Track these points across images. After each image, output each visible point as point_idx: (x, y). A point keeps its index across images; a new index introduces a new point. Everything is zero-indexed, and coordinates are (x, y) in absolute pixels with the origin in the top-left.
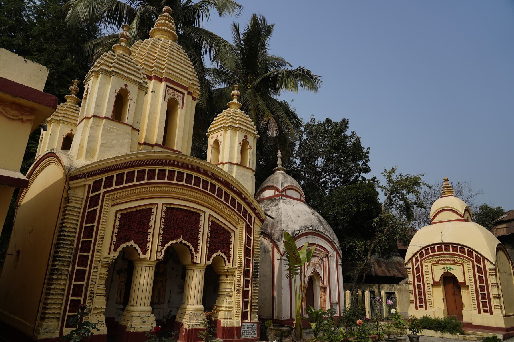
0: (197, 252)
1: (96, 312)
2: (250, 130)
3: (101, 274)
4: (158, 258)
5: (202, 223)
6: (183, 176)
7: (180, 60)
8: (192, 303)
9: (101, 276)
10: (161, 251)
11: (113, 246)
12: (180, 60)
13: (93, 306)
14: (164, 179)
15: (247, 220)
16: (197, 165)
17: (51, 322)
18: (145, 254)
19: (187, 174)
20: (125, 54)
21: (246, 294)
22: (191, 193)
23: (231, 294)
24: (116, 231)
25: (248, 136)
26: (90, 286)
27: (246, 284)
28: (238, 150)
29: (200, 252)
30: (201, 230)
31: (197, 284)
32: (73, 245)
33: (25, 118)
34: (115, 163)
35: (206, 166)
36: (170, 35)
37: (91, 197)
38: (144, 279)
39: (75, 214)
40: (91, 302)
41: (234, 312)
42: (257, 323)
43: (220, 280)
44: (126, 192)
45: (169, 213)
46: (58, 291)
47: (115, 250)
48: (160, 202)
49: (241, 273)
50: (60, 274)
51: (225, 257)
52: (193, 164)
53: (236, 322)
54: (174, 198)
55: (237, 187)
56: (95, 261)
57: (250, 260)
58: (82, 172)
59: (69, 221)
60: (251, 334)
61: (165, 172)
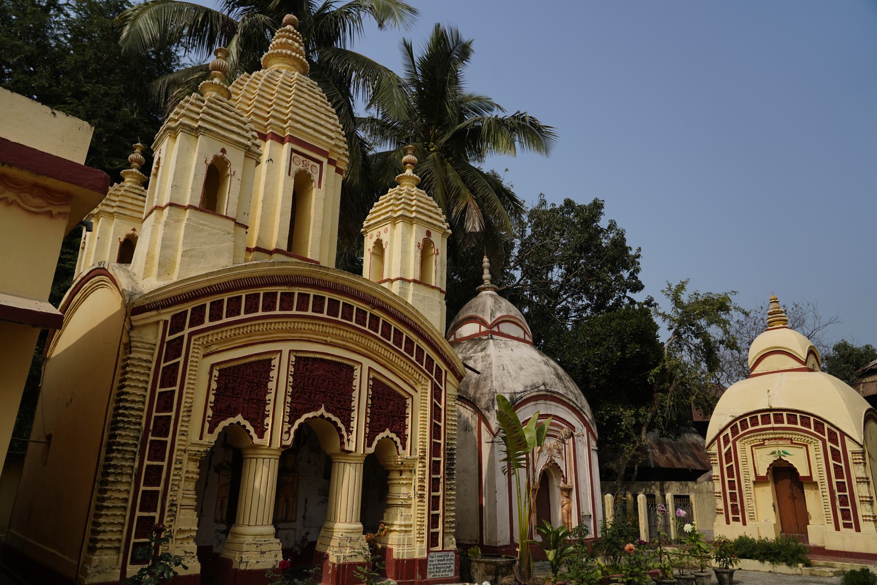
0: (349, 431)
1: (181, 536)
2: (435, 222)
3: (187, 472)
4: (284, 443)
5: (356, 383)
6: (323, 303)
7: (314, 106)
8: (343, 520)
9: (187, 475)
10: (288, 432)
11: (207, 425)
12: (314, 106)
13: (175, 527)
14: (291, 309)
15: (433, 377)
16: (347, 283)
17: (106, 555)
18: (261, 436)
20: (222, 98)
21: (434, 503)
22: (338, 332)
23: (409, 502)
24: (212, 398)
26: (169, 493)
27: (434, 485)
28: (416, 256)
30: (355, 394)
31: (351, 487)
32: (140, 424)
33: (55, 210)
34: (208, 284)
35: (361, 285)
38: (261, 479)
39: (142, 371)
40: (172, 520)
41: (414, 533)
42: (455, 551)
43: (389, 480)
44: (228, 332)
45: (301, 366)
46: (117, 501)
47: (211, 431)
48: (286, 347)
52: (340, 282)
53: (418, 550)
54: (309, 341)
55: (416, 321)
56: (178, 450)
58: (152, 300)
59: (132, 384)
60: (445, 571)
61: (293, 297)
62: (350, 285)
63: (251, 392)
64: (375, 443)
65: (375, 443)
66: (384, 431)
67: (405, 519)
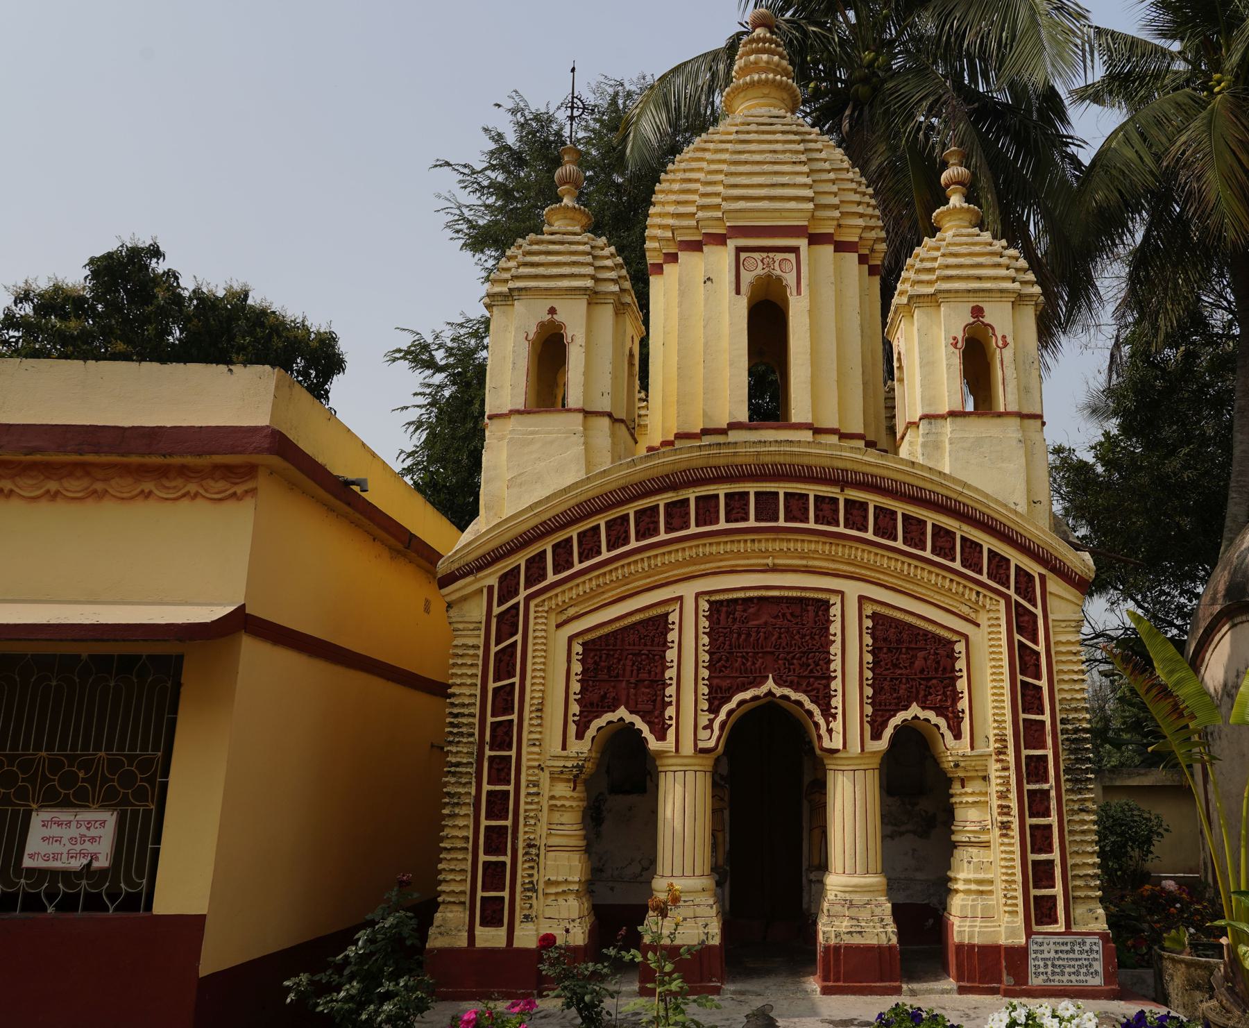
0: (828, 714)
1: (553, 890)
3: (552, 798)
4: (701, 745)
5: (835, 628)
7: (769, 157)
9: (553, 802)
10: (709, 726)
11: (572, 728)
12: (769, 157)
13: (541, 878)
14: (688, 527)
15: (1012, 592)
16: (782, 459)
18: (661, 737)
19: (756, 493)
21: (1039, 839)
22: (784, 546)
23: (984, 838)
24: (576, 687)
25: (987, 307)
26: (521, 828)
27: (1036, 803)
28: (949, 366)
29: (840, 717)
30: (835, 649)
32: (472, 735)
33: (239, 489)
35: (809, 454)
36: (766, 91)
37: (500, 616)
38: (683, 806)
39: (469, 662)
40: (532, 868)
41: (997, 899)
42: (1103, 936)
47: (580, 736)
48: (688, 591)
49: (1006, 769)
50: (458, 804)
51: (942, 723)
52: (768, 459)
56: (529, 768)
57: (1043, 722)
58: (462, 562)
59: (458, 681)
60: (1077, 973)
62: (788, 460)
63: (639, 669)
64: (888, 732)
65: (888, 732)
66: (906, 708)
67: (976, 870)
